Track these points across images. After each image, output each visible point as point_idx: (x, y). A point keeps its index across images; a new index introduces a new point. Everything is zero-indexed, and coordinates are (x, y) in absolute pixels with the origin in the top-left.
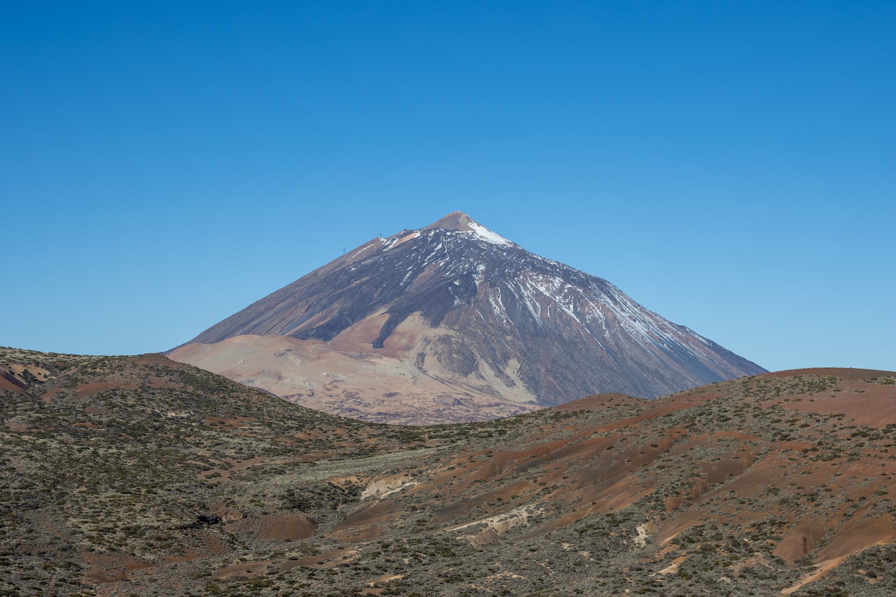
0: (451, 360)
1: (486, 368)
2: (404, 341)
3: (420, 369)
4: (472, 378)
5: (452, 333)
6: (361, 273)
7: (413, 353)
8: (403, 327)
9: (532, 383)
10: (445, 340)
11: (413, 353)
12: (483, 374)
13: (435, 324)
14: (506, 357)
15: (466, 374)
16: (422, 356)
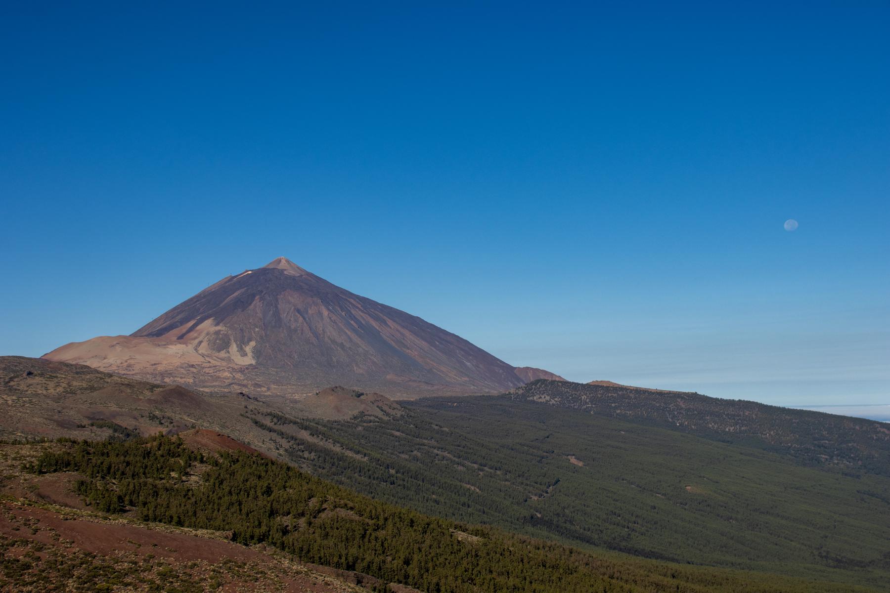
0: (214, 343)
1: (234, 348)
2: (196, 335)
3: (196, 350)
4: (223, 354)
5: (224, 328)
6: (205, 297)
7: (197, 341)
8: (199, 327)
9: (257, 353)
10: (217, 333)
11: (197, 341)
12: (230, 350)
13: (217, 324)
14: (250, 340)
15: (219, 351)
16: (201, 342)
